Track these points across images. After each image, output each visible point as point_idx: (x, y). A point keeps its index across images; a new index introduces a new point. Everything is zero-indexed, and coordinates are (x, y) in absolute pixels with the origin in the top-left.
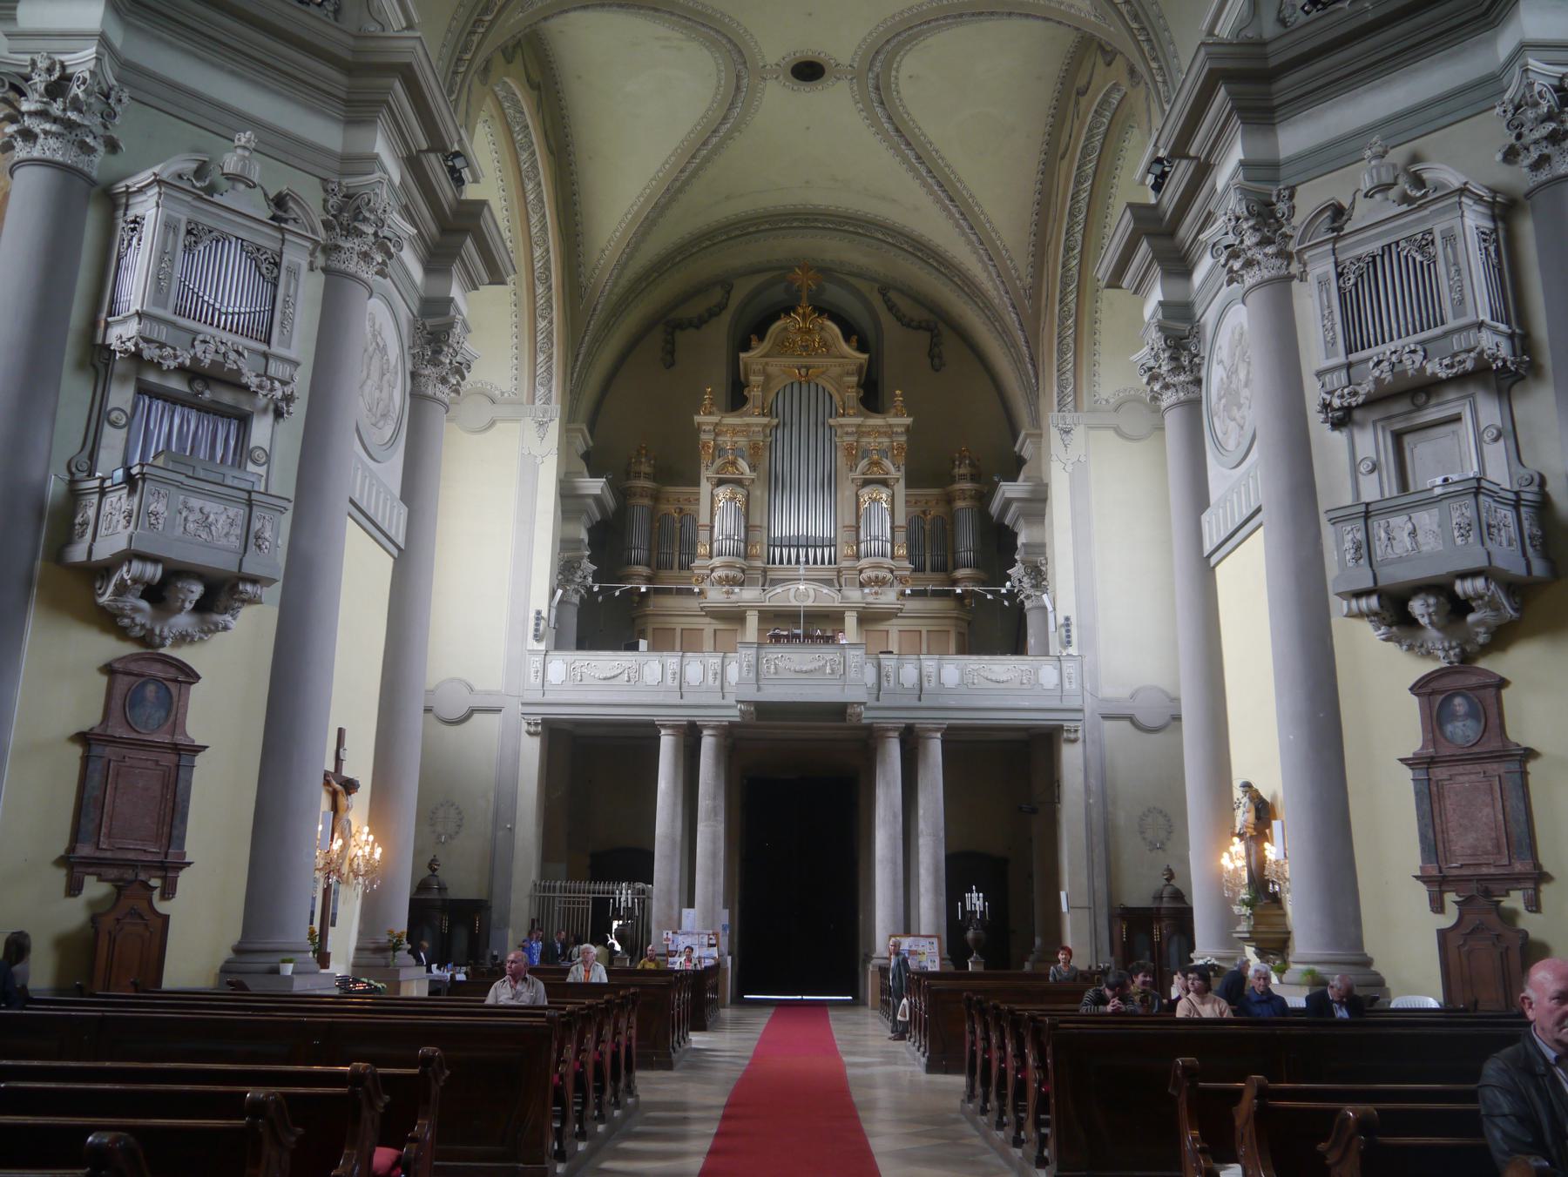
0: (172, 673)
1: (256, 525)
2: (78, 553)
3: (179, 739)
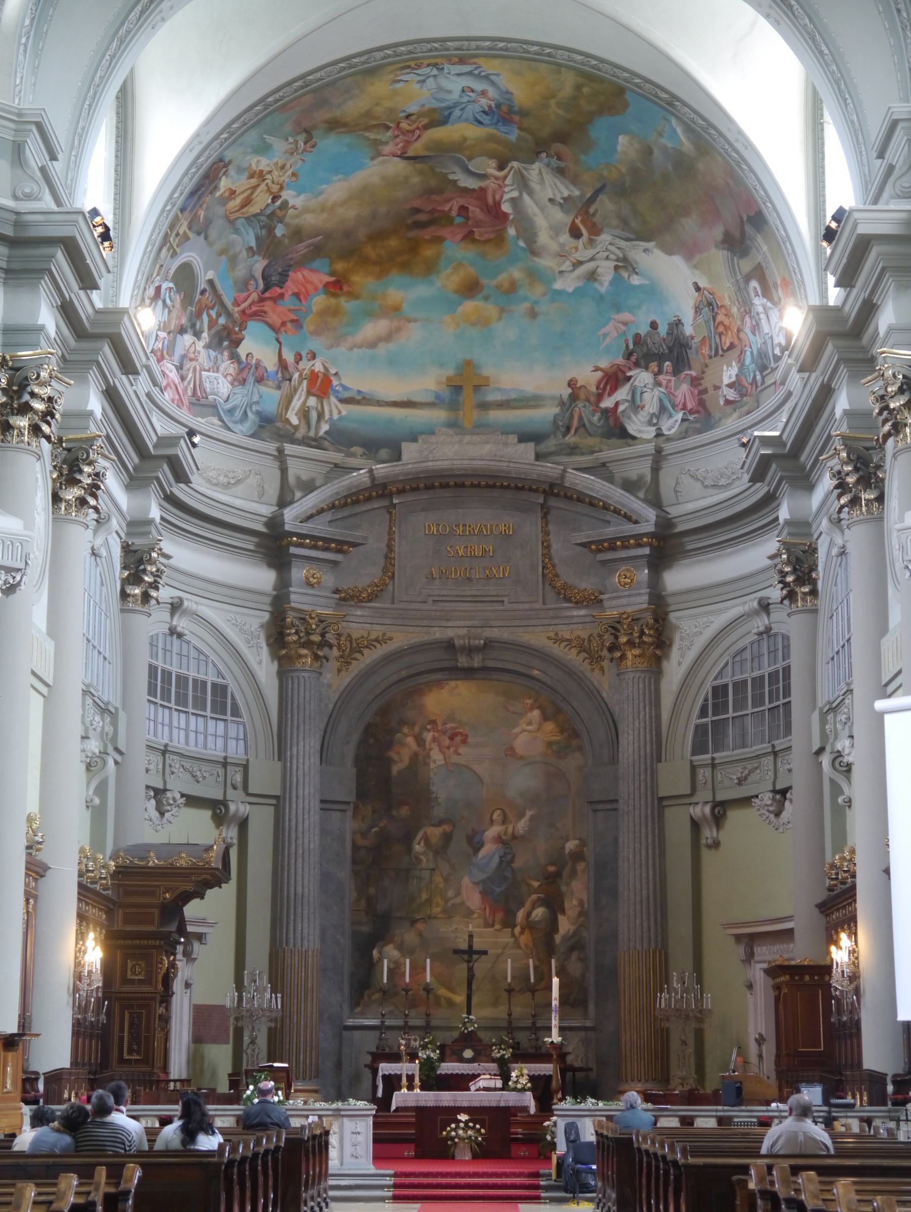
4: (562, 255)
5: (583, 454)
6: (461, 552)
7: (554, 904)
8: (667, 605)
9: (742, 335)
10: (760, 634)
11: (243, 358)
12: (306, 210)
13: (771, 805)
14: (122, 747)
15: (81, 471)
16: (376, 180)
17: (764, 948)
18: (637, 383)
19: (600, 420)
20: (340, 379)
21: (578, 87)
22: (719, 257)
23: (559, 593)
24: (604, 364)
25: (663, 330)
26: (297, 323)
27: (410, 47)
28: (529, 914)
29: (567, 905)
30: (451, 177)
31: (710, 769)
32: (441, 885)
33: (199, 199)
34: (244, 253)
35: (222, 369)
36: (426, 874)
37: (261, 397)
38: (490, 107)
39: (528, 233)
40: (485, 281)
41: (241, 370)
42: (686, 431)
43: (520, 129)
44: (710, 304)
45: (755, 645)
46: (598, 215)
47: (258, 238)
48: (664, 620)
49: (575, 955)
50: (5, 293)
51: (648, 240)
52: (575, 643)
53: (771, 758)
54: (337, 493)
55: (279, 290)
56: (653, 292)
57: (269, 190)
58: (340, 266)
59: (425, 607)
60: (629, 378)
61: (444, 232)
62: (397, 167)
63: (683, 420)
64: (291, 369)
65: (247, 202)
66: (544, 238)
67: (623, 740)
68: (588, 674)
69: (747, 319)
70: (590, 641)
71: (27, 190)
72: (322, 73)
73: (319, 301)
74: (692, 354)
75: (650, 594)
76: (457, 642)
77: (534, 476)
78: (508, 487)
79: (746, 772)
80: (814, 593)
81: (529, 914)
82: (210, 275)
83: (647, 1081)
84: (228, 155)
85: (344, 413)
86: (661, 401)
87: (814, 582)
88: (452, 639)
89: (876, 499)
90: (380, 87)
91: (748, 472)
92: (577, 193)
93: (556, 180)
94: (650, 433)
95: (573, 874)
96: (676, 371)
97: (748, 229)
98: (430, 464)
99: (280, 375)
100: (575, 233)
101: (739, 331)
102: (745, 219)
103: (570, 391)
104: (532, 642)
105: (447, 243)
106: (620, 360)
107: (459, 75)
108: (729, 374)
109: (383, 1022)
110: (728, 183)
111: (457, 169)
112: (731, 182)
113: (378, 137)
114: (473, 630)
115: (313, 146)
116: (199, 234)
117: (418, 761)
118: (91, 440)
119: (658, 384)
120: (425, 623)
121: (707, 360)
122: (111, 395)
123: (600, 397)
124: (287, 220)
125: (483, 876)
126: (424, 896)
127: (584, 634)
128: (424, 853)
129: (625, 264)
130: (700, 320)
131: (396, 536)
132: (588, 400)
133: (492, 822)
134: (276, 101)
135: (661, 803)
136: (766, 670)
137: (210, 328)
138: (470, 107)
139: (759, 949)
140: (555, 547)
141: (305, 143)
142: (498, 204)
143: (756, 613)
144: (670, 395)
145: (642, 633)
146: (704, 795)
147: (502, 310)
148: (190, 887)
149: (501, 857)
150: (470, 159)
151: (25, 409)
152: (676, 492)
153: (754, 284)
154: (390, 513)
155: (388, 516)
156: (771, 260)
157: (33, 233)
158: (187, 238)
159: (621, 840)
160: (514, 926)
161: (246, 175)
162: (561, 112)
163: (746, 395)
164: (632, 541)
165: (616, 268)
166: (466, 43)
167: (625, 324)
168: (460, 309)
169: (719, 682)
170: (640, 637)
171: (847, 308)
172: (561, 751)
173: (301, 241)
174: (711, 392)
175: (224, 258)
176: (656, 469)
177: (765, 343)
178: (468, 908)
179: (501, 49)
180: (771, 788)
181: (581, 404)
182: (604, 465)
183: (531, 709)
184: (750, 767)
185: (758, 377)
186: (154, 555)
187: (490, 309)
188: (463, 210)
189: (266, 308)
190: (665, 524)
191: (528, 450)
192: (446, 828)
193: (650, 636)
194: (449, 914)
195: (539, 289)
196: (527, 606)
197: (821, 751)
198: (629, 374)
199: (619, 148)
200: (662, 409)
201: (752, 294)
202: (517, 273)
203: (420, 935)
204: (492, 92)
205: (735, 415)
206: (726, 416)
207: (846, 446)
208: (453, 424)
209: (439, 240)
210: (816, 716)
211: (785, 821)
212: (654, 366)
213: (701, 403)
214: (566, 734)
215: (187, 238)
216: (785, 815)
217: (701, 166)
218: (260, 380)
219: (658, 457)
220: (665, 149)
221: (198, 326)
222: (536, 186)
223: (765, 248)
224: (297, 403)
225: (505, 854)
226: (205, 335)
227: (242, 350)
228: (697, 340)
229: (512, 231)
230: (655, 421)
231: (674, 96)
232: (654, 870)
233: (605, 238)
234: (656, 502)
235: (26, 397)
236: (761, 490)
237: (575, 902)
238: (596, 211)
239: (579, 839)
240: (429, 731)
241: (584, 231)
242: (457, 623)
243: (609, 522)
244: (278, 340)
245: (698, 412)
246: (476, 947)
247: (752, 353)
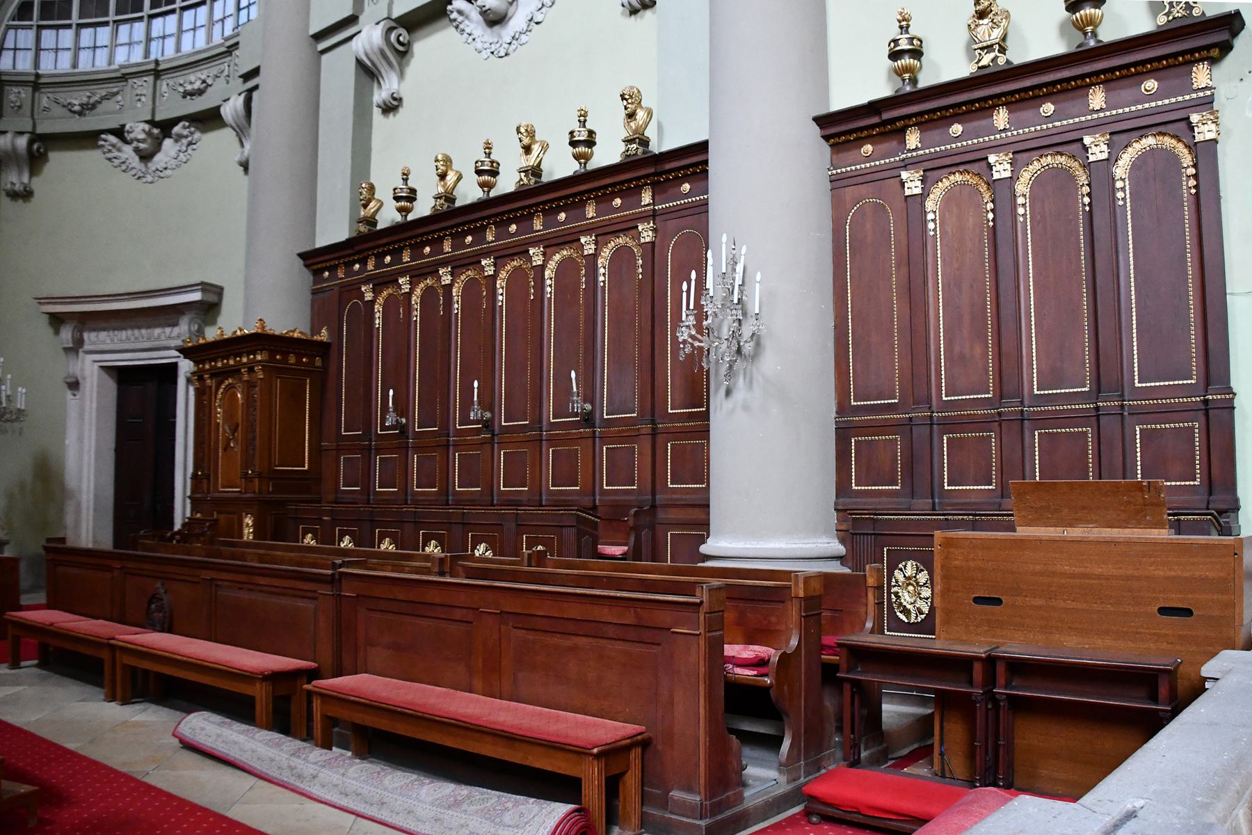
13: (143, 141)
31: (30, 89)
53: (150, 79)
79: (96, 98)
139: (93, 335)
180: (149, 118)
184: (104, 93)
197: (352, 20)
211: (161, 166)
216: (160, 159)
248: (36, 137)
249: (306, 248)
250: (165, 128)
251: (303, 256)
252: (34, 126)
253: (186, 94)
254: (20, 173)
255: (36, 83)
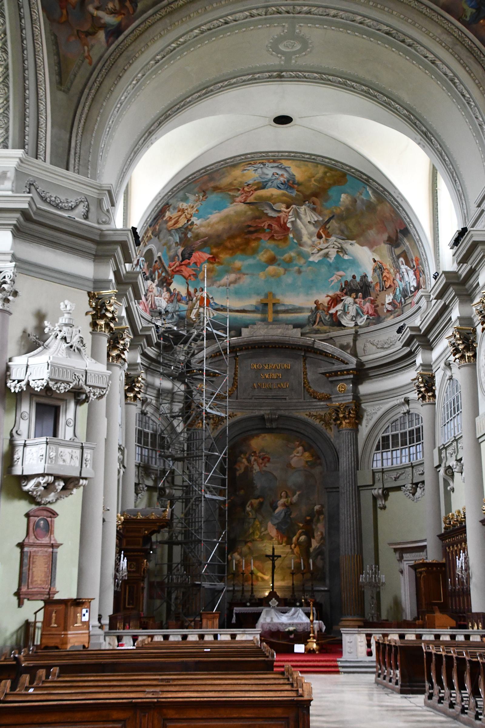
0: (50, 514)
1: (85, 455)
2: (18, 471)
3: (52, 542)
4: (313, 246)
5: (321, 333)
6: (267, 377)
7: (310, 534)
8: (361, 400)
9: (395, 282)
10: (404, 413)
11: (172, 291)
12: (201, 226)
14: (126, 466)
15: (119, 343)
16: (232, 213)
17: (408, 555)
18: (346, 302)
19: (329, 318)
20: (213, 300)
21: (325, 173)
22: (385, 248)
23: (311, 395)
24: (331, 294)
25: (358, 279)
26: (196, 276)
27: (253, 155)
28: (298, 539)
29: (315, 534)
30: (265, 212)
32: (259, 526)
33: (157, 221)
34: (174, 245)
35: (163, 295)
36: (252, 521)
37: (179, 308)
38: (285, 181)
39: (298, 236)
40: (278, 257)
41: (171, 296)
42: (369, 323)
43: (297, 191)
44: (380, 268)
45: (402, 419)
46: (330, 229)
47: (180, 238)
48: (359, 407)
49: (319, 557)
50: (95, 266)
51: (352, 240)
52: (318, 417)
53: (411, 469)
54: (213, 351)
55: (188, 261)
56: (354, 262)
57: (186, 217)
58: (215, 250)
59: (251, 401)
60: (343, 300)
61: (261, 236)
62: (242, 207)
63: (367, 319)
64: (192, 296)
65: (176, 222)
66: (305, 238)
67: (341, 460)
68: (324, 431)
69: (398, 274)
70: (325, 416)
71: (104, 220)
72: (213, 166)
73: (206, 266)
74: (371, 290)
75: (353, 396)
76: (266, 417)
77: (301, 343)
78: (295, 348)
79: (398, 475)
80: (434, 396)
81: (298, 539)
82: (159, 254)
83: (354, 615)
84: (171, 202)
85: (215, 315)
86: (357, 310)
87: (434, 391)
88: (263, 415)
89: (473, 356)
90: (237, 172)
91: (402, 342)
92: (321, 219)
93: (312, 213)
94: (352, 324)
95: (318, 521)
96: (364, 297)
97: (400, 236)
98: (254, 338)
99: (188, 298)
100: (320, 237)
101: (394, 280)
102: (398, 231)
103: (315, 305)
104: (299, 416)
105: (262, 241)
106: (338, 292)
107: (272, 167)
108: (389, 298)
109: (234, 588)
110: (391, 215)
111: (268, 208)
112: (393, 215)
113: (234, 194)
114: (272, 411)
115: (206, 198)
116: (156, 236)
117: (248, 470)
118: (123, 330)
119: (355, 303)
120: (251, 408)
121: (378, 293)
122: (129, 310)
123: (329, 308)
124: (193, 230)
125: (277, 522)
126: (251, 531)
127: (322, 413)
128: (250, 511)
129: (341, 250)
130: (376, 274)
131: (238, 370)
132: (324, 310)
133: (281, 497)
134: (193, 178)
135: (358, 489)
136: (408, 429)
137: (158, 277)
138: (275, 181)
140: (309, 374)
141: (203, 197)
142: (285, 224)
143: (403, 404)
144: (361, 308)
145: (350, 413)
146: (379, 485)
147: (286, 270)
148: (156, 529)
149: (285, 513)
150: (274, 204)
151: (104, 316)
152: (364, 350)
153: (401, 259)
154: (236, 359)
155: (234, 361)
156: (411, 250)
157: (108, 239)
158: (151, 238)
159: (341, 505)
160: (291, 544)
161: (177, 211)
162: (317, 184)
163: (397, 308)
164: (345, 372)
165: (338, 252)
166: (277, 154)
167: (341, 276)
168: (267, 269)
169: (385, 434)
170: (349, 414)
171: (460, 272)
172: (312, 465)
173: (198, 239)
174: (380, 306)
175: (165, 247)
176: (355, 341)
177: (406, 285)
178: (271, 536)
179: (292, 156)
181: (320, 312)
182: (331, 338)
183: (298, 447)
184: (400, 473)
185: (403, 300)
186: (140, 379)
187: (281, 270)
188: (270, 226)
189: (182, 269)
190: (360, 364)
191: (297, 332)
192: (261, 500)
193: (353, 414)
194: (262, 538)
195: (302, 261)
196: (296, 401)
198: (342, 298)
199: (342, 200)
200: (358, 314)
201: (400, 264)
202: (293, 254)
203: (249, 548)
204: (286, 175)
205: (392, 316)
206: (387, 317)
207: (459, 332)
208: (264, 320)
209: (259, 239)
210: (436, 451)
212: (354, 295)
213: (376, 311)
214: (314, 458)
215: (151, 238)
216: (417, 494)
217: (379, 208)
218: (179, 301)
219: (356, 335)
220: (363, 199)
221: (153, 276)
222: (303, 216)
223: (408, 244)
224: (195, 311)
225: (287, 511)
226: (156, 281)
227: (172, 287)
228: (374, 283)
229: (291, 236)
230: (354, 319)
231: (369, 177)
232: (356, 519)
233: (333, 239)
234: (355, 354)
235: (104, 311)
236: (407, 350)
237: (319, 533)
238: (329, 227)
239: (321, 505)
240: (253, 456)
241: (324, 236)
242: (266, 408)
243: (334, 364)
244: (187, 283)
245: (374, 315)
246: (276, 553)
247: (400, 290)
248: (384, 489)
249: (439, 534)
250: (417, 484)
251: (439, 536)
252: (383, 486)
253: (419, 474)
254: (382, 501)
255: (383, 471)
